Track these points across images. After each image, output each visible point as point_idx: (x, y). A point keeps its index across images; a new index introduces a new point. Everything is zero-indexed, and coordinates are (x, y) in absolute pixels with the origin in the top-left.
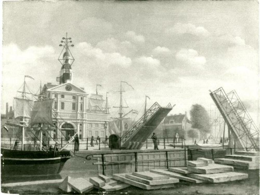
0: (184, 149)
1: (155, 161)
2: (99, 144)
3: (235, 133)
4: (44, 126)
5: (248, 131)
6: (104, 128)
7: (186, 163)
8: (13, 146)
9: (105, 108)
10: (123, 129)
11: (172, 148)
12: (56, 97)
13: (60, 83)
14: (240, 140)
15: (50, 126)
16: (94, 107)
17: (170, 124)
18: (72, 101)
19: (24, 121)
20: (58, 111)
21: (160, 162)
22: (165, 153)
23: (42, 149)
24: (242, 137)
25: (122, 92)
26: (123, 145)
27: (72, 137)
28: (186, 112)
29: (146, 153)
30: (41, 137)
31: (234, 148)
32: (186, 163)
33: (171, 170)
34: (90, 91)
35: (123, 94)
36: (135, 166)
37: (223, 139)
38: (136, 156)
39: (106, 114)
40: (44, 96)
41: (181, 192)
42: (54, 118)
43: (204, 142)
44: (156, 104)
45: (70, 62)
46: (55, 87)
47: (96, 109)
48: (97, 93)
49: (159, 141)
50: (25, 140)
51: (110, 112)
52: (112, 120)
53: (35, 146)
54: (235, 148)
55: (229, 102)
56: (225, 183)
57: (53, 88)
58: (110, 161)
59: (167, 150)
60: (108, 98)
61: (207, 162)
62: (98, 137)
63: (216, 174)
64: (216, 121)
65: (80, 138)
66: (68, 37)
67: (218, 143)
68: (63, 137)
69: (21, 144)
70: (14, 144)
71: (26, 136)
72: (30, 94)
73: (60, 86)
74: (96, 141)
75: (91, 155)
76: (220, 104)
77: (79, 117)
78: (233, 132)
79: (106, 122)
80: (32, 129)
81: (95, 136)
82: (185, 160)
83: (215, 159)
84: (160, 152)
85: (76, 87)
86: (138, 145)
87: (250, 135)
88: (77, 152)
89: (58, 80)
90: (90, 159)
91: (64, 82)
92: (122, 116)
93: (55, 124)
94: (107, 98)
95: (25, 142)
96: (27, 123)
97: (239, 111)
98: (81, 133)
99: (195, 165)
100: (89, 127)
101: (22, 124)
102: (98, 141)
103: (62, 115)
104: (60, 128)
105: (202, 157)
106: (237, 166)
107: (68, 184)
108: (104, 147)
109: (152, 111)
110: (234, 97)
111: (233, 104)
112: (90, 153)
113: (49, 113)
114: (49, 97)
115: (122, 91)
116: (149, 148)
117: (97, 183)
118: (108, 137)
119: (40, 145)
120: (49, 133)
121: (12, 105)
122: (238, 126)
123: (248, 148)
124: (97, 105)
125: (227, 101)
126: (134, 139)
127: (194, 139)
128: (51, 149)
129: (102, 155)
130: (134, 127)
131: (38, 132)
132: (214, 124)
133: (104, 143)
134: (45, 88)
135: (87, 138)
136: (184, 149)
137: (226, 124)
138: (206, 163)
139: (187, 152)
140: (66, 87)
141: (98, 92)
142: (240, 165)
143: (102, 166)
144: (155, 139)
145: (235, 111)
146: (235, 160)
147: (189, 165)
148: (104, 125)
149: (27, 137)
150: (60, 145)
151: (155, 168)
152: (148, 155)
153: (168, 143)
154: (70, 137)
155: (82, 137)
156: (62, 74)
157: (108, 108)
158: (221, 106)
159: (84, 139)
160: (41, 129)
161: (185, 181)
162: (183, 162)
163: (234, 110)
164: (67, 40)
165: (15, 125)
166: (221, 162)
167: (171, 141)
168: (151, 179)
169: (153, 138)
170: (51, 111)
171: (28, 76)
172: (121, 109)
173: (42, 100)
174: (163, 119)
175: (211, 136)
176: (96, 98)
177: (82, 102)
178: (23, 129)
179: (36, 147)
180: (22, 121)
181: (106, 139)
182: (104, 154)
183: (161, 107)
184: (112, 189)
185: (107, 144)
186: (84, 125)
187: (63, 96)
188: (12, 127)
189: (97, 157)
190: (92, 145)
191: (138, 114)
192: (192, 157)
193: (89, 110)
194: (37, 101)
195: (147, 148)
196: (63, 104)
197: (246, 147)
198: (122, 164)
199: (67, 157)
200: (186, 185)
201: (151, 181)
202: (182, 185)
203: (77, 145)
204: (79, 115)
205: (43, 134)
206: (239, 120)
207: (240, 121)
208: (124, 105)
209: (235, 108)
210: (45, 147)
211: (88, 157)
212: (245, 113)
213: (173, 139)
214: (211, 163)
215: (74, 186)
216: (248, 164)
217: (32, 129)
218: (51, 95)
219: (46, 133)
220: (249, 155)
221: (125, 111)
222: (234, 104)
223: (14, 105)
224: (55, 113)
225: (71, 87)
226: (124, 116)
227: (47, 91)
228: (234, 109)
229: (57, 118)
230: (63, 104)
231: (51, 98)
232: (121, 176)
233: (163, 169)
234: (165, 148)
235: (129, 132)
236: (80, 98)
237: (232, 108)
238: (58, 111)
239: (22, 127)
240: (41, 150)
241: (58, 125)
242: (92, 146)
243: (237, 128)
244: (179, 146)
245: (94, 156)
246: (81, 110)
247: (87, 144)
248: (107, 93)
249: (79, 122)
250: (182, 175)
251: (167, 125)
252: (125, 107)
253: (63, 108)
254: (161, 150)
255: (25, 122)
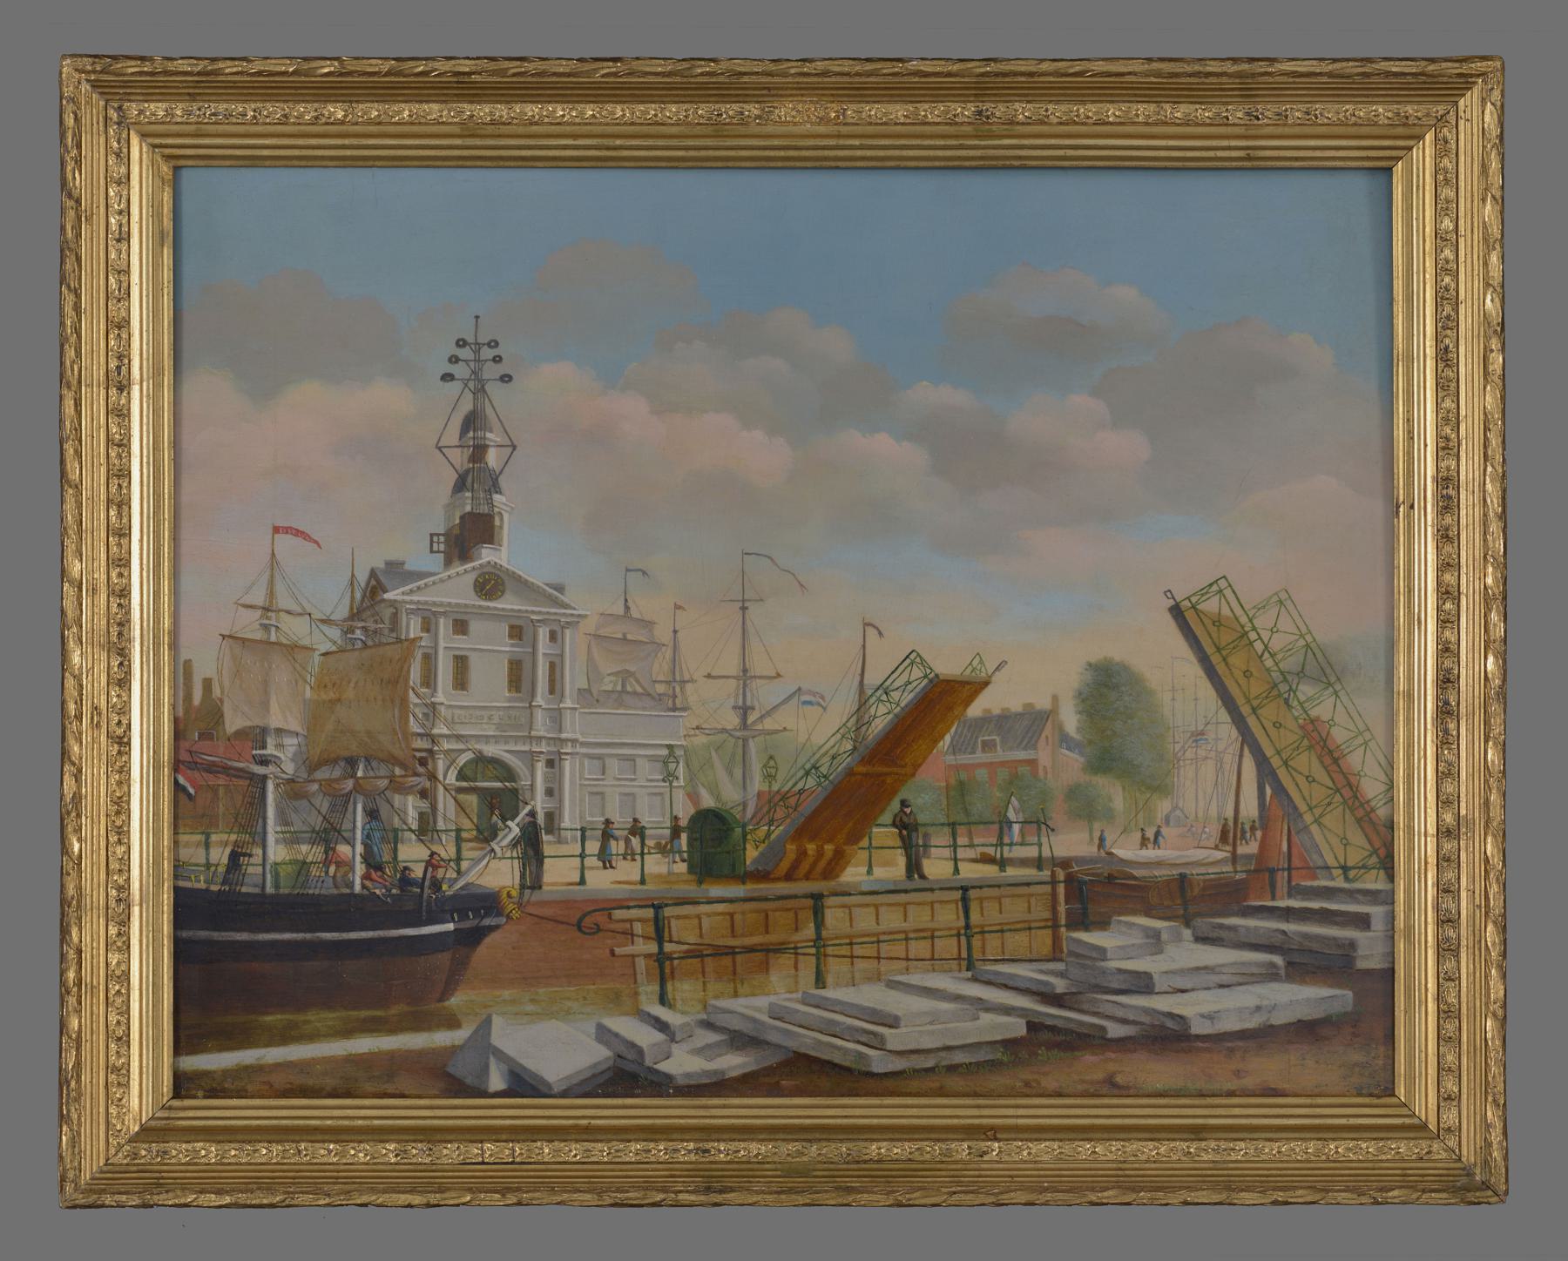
0: (1046, 874)
1: (912, 935)
2: (638, 858)
3: (1288, 795)
4: (372, 774)
5: (1349, 784)
6: (664, 780)
7: (1056, 940)
8: (221, 869)
9: (667, 682)
10: (757, 784)
11: (990, 871)
12: (428, 631)
13: (448, 563)
14: (1314, 829)
15: (403, 773)
16: (612, 678)
17: (980, 757)
18: (506, 646)
19: (270, 750)
20: (440, 697)
21: (933, 937)
22: (958, 895)
23: (364, 887)
24: (1321, 816)
25: (747, 604)
26: (755, 861)
27: (509, 823)
28: (1055, 699)
29: (868, 899)
30: (359, 824)
31: (1283, 869)
32: (1056, 940)
33: (986, 977)
34: (582, 601)
35: (754, 612)
36: (813, 960)
37: (1231, 823)
38: (818, 914)
39: (674, 709)
40: (371, 625)
41: (1034, 1084)
42: (420, 731)
43: (1144, 842)
44: (912, 658)
45: (492, 458)
46: (421, 583)
47: (623, 686)
48: (627, 608)
49: (926, 836)
50: (277, 842)
51: (692, 700)
52: (701, 740)
53: (327, 873)
54: (1289, 869)
55: (1259, 646)
56: (1243, 1035)
57: (413, 586)
58: (692, 940)
59: (969, 879)
60: (679, 634)
61: (1156, 935)
62: (635, 820)
63: (1202, 995)
64: (1198, 737)
65: (549, 831)
66: (483, 339)
67: (1212, 843)
68: (464, 827)
69: (259, 860)
70: (225, 860)
71: (283, 819)
72: (301, 614)
73: (444, 575)
74: (627, 841)
75: (603, 909)
76: (1215, 659)
77: (541, 726)
78: (1280, 789)
79: (670, 747)
80: (315, 787)
81: (621, 821)
82: (1055, 926)
83: (1198, 922)
84: (932, 890)
85: (526, 583)
86: (810, 860)
87: (1362, 805)
88: (536, 896)
89: (435, 547)
90: (598, 929)
91: (465, 556)
92: (751, 718)
93: (423, 762)
94: (675, 632)
95: (277, 852)
96: (286, 755)
97: (1306, 690)
98: (550, 805)
99: (1102, 952)
100: (589, 774)
101: (264, 761)
102: (635, 841)
103: (457, 720)
104: (447, 782)
105: (1134, 912)
106: (1301, 951)
107: (493, 1053)
108: (664, 869)
109: (895, 695)
110: (1285, 624)
111: (1279, 657)
112: (595, 901)
113: (396, 711)
114: (392, 630)
115: (749, 600)
116: (879, 872)
117: (632, 1045)
118: (684, 823)
119: (352, 869)
120: (396, 804)
121: (210, 672)
122: (1307, 762)
123: (1354, 868)
124: (632, 669)
125: (1251, 644)
126: (807, 829)
127: (1097, 826)
128: (405, 881)
129: (658, 908)
130: (807, 773)
131: (342, 803)
132: (1189, 754)
133: (662, 849)
134: (374, 588)
135: (583, 830)
136: (1045, 874)
137: (1246, 751)
138: (1155, 942)
139: (1061, 889)
140: (476, 580)
141: (630, 604)
142: (1315, 946)
143: (658, 960)
144: (906, 827)
145: (1291, 689)
146: (1291, 927)
147: (1071, 953)
148: (665, 763)
149: (286, 829)
150: (452, 864)
151: (911, 970)
152: (877, 907)
153: (971, 846)
154: (500, 824)
155: (556, 822)
156: (458, 515)
157: (683, 682)
158: (1221, 668)
159: (569, 833)
160: (358, 789)
161: (1052, 1029)
162: (1044, 939)
163: (1280, 690)
164: (477, 352)
165: (226, 770)
166: (1224, 934)
167: (985, 841)
168: (893, 1023)
169: (898, 823)
170: (404, 701)
171: (287, 530)
172: (745, 686)
173: (359, 645)
174: (948, 730)
175: (1178, 812)
176: (624, 635)
177: (557, 655)
178: (270, 786)
179: (334, 877)
180: (264, 747)
181: (676, 832)
182: (667, 905)
183: (937, 676)
184: (706, 1073)
185: (677, 858)
186: (567, 765)
187: (461, 627)
188: (212, 780)
189: (631, 921)
190: (604, 863)
191: (825, 709)
192: (1085, 914)
193: (589, 691)
194: (334, 648)
195: (869, 872)
196: (461, 663)
197: (1342, 862)
198: (751, 950)
199: (487, 922)
200: (1058, 1046)
201: (893, 1031)
202: (1042, 1051)
203: (534, 861)
204: (539, 716)
205: (364, 809)
206: (1306, 735)
207: (1316, 737)
208: (759, 665)
209: (1289, 678)
210: (379, 873)
211: (588, 921)
212: (1337, 696)
213: (996, 827)
214: (1178, 939)
215: (524, 1062)
216: (1352, 945)
217: (315, 787)
218: (404, 619)
219: (384, 811)
220: (1358, 902)
221: (766, 695)
222: (1284, 659)
223: (220, 672)
224: (426, 711)
225: (503, 584)
226: (762, 717)
227: (384, 600)
228: (1285, 680)
229: (435, 731)
230: (461, 663)
231: (403, 637)
232: (746, 1007)
233: (950, 974)
234: (957, 870)
235: (784, 797)
236: (543, 633)
237: (1276, 675)
238: (440, 697)
239: (264, 778)
240: (358, 888)
241: (441, 765)
242: (605, 868)
243: (1296, 770)
244: (1024, 862)
245: (618, 914)
246: (552, 692)
247: (582, 856)
248: (677, 607)
249: (542, 753)
250: (1039, 998)
251: (964, 759)
252: (761, 677)
253: (461, 682)
254: (937, 881)
255: (275, 753)
